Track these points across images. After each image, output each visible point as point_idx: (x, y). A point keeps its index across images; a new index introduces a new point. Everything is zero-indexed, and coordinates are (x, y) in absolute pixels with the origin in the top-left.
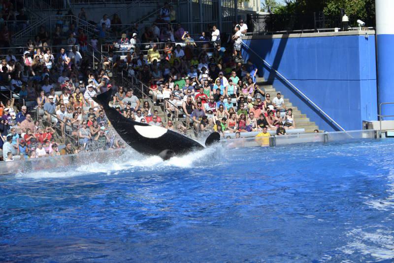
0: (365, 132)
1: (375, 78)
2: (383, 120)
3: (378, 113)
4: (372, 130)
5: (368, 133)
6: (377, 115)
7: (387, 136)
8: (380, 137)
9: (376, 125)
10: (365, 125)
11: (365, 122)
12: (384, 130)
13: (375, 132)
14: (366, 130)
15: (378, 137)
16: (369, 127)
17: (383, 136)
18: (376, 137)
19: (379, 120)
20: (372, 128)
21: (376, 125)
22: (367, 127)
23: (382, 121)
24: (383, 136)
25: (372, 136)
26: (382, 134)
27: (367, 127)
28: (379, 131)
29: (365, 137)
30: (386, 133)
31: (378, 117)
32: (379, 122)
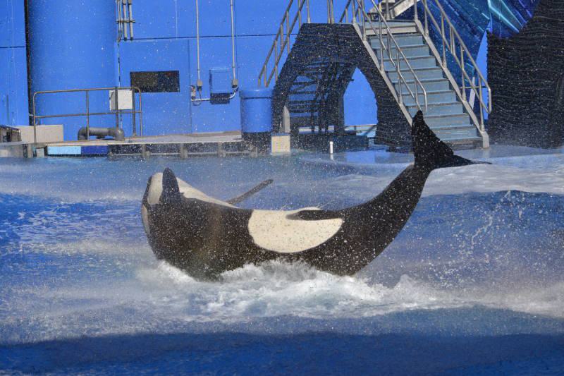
0: (5, 147)
1: (24, 44)
2: (39, 124)
3: (31, 112)
4: (17, 143)
5: (11, 148)
6: (28, 115)
7: (46, 154)
8: (35, 155)
9: (27, 134)
10: (5, 134)
11: (4, 128)
12: (42, 144)
13: (25, 147)
14: (6, 144)
15: (30, 155)
16: (14, 137)
17: (41, 153)
18: (25, 155)
19: (31, 124)
20: (19, 140)
21: (27, 134)
22: (9, 138)
23: (38, 127)
24: (41, 153)
25: (18, 153)
26: (38, 150)
27: (9, 138)
28: (32, 144)
29: (6, 156)
30: (46, 149)
31: (31, 119)
32: (32, 127)
